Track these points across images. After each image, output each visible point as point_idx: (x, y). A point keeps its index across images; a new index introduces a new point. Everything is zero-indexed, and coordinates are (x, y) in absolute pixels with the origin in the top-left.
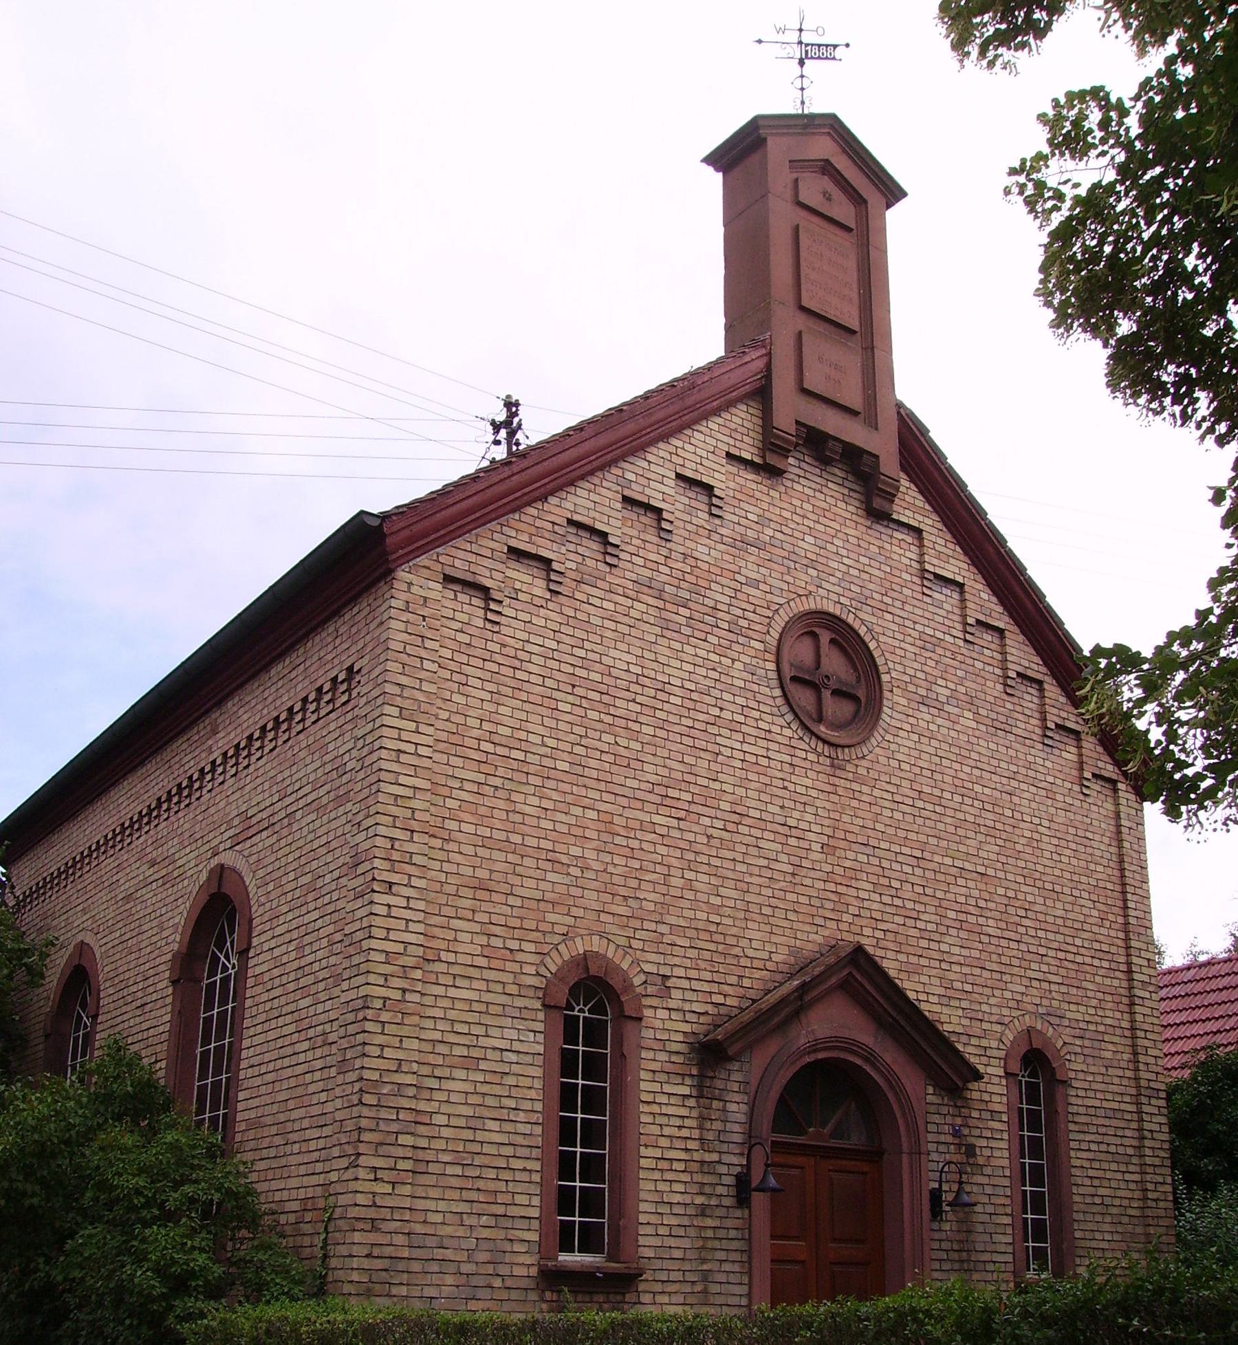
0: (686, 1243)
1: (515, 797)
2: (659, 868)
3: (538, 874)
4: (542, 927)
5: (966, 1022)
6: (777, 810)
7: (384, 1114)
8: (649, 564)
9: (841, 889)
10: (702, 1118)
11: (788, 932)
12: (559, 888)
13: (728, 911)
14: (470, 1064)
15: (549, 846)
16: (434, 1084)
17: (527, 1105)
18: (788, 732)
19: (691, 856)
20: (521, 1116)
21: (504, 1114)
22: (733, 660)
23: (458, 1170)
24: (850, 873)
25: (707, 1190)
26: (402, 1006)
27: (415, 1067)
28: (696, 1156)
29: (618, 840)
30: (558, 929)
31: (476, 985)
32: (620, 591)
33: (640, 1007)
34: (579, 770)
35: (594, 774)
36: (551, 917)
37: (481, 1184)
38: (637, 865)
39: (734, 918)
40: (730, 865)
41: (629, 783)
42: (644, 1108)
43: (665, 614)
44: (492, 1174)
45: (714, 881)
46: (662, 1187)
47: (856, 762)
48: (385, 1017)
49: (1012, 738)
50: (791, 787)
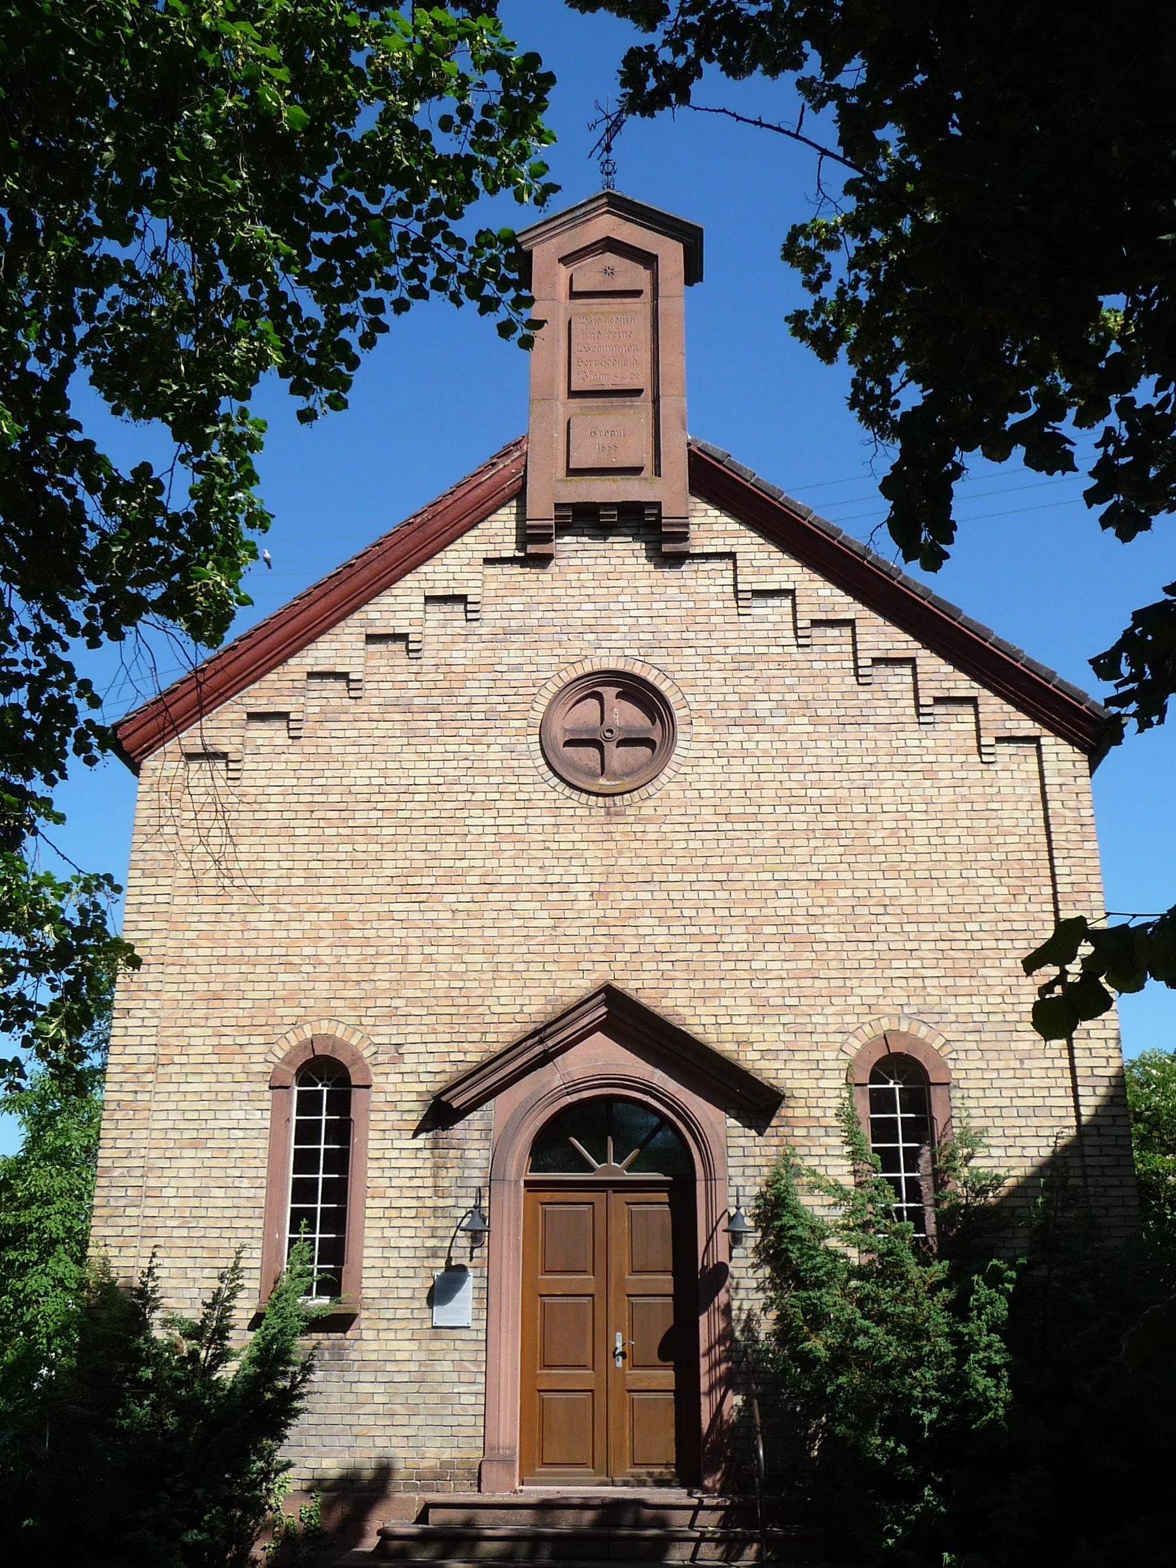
0: (416, 1283)
1: (249, 917)
2: (396, 950)
3: (269, 977)
4: (271, 1021)
5: (791, 1037)
6: (536, 871)
7: (114, 1192)
8: (398, 685)
9: (613, 931)
10: (437, 1167)
11: (544, 983)
12: (288, 986)
13: (473, 975)
14: (197, 1143)
15: (282, 951)
16: (166, 1164)
17: (252, 1173)
18: (554, 795)
19: (433, 933)
20: (245, 1183)
21: (229, 1181)
22: (489, 745)
23: (184, 1232)
24: (625, 914)
25: (440, 1233)
26: (133, 1105)
27: (143, 1152)
28: (428, 1203)
29: (352, 933)
30: (286, 1020)
31: (206, 1078)
32: (365, 717)
33: (368, 1074)
34: (314, 882)
35: (330, 882)
36: (280, 1012)
37: (204, 1242)
38: (372, 951)
39: (480, 981)
40: (479, 932)
41: (366, 881)
42: (370, 1164)
43: (412, 725)
44: (216, 1233)
45: (457, 950)
46: (388, 1233)
47: (640, 804)
48: (119, 1115)
49: (870, 728)
50: (554, 846)
